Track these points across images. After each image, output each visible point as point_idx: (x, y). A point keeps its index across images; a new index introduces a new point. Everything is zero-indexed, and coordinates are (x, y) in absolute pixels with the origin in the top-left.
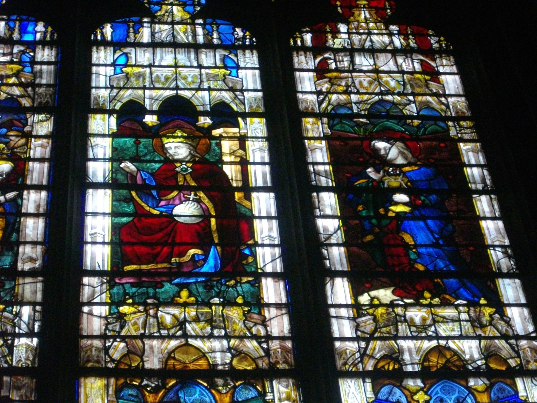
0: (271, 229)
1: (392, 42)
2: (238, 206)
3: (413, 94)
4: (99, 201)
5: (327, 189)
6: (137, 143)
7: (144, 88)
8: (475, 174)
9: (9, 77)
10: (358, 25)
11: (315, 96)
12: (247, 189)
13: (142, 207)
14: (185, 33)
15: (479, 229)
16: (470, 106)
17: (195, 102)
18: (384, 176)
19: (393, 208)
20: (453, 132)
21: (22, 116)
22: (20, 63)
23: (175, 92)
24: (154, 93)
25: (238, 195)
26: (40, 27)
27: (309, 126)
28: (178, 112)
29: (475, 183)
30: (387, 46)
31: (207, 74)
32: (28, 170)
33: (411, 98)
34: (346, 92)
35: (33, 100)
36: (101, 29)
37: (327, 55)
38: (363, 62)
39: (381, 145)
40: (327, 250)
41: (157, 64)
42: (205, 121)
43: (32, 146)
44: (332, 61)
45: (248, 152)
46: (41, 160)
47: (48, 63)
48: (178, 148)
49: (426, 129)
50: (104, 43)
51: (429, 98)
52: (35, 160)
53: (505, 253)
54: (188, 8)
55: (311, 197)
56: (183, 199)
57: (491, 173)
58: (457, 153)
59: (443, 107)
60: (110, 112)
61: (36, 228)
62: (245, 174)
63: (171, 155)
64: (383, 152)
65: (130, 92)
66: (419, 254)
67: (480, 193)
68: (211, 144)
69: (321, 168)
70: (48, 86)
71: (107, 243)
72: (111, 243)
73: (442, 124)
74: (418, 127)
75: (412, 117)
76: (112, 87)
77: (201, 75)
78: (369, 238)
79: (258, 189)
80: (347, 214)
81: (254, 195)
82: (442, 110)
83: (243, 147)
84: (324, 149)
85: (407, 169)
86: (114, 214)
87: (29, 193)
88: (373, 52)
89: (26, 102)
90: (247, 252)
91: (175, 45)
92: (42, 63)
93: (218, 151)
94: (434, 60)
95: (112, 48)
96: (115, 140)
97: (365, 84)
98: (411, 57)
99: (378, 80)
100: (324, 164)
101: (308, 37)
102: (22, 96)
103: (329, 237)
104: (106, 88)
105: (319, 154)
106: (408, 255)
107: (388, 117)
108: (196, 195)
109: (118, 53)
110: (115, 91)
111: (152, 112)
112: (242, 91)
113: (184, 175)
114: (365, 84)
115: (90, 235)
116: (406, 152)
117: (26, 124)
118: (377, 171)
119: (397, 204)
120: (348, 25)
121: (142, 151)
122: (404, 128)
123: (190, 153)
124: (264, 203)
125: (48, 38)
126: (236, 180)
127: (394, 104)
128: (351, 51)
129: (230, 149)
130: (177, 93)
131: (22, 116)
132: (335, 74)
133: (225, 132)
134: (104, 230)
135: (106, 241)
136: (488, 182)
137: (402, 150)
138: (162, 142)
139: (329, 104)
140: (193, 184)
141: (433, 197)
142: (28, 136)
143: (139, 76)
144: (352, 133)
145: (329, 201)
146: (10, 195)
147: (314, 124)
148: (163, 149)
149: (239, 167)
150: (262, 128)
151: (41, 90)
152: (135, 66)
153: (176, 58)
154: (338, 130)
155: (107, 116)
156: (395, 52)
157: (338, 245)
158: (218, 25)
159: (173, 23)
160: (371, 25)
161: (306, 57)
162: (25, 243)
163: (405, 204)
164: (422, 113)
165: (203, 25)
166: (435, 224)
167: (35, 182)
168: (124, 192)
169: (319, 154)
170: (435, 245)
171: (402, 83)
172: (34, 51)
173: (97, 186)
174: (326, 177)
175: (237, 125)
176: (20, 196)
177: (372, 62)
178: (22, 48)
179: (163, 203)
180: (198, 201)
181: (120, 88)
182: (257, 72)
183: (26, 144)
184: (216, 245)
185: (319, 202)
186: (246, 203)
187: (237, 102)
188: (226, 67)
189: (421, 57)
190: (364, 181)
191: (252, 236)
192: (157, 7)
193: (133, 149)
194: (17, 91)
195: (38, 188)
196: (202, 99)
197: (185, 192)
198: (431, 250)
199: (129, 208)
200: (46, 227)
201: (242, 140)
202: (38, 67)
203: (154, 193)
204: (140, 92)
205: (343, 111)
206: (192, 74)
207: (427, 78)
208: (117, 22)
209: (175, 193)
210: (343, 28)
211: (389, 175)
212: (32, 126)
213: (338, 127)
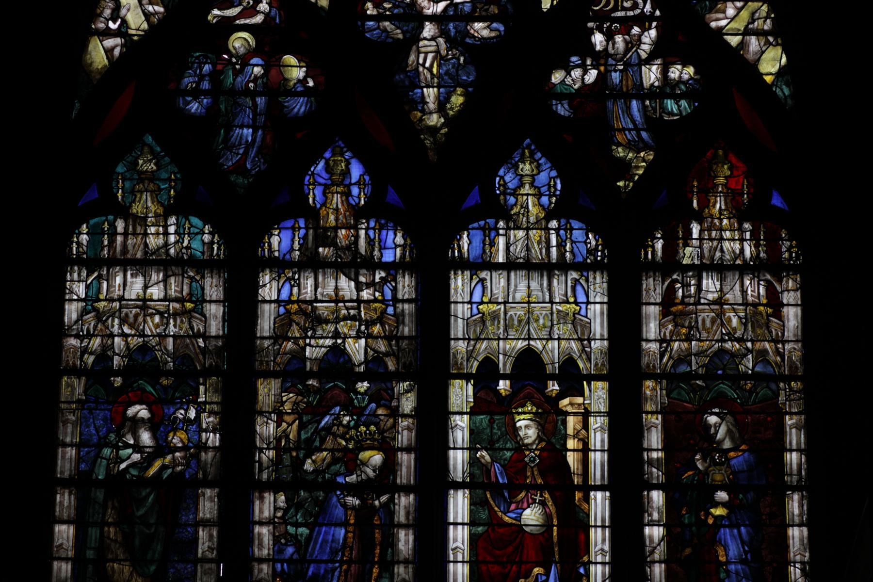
0: (604, 540)
1: (742, 250)
2: (577, 509)
3: (752, 341)
4: (459, 505)
5: (657, 487)
6: (491, 422)
7: (499, 339)
8: (793, 458)
9: (373, 323)
10: (712, 222)
11: (658, 344)
12: (587, 488)
13: (495, 511)
14: (539, 243)
15: (785, 537)
16: (805, 358)
17: (546, 358)
18: (710, 466)
19: (712, 510)
20: (782, 398)
21: (389, 385)
22: (383, 301)
23: (526, 343)
24: (509, 345)
25: (578, 495)
26: (399, 240)
27: (648, 392)
28: (529, 363)
29: (791, 475)
30: (736, 258)
31: (559, 311)
32: (398, 463)
33: (749, 345)
34: (688, 339)
35: (398, 359)
36: (459, 241)
37: (675, 277)
38: (710, 285)
39: (713, 419)
40: (650, 568)
41: (510, 300)
42: (553, 387)
43: (400, 429)
44: (679, 285)
45: (590, 443)
46: (407, 450)
47: (409, 301)
48: (527, 428)
49: (757, 394)
50: (463, 264)
51: (767, 345)
52: (402, 450)
53: (803, 570)
54: (545, 200)
55: (642, 496)
56: (530, 501)
57: (807, 461)
58: (780, 431)
59: (778, 358)
60: (467, 377)
61: (407, 542)
62: (585, 462)
63: (521, 439)
64: (713, 430)
65: (485, 344)
66: (728, 572)
67: (794, 489)
68: (557, 420)
69: (654, 455)
70: (409, 338)
71: (467, 562)
72: (470, 562)
73: (773, 386)
74: (750, 391)
75: (745, 376)
76: (469, 339)
77: (552, 308)
78: (688, 551)
79: (597, 488)
80: (671, 523)
81: (592, 493)
82: (776, 363)
83: (586, 426)
84: (660, 427)
85: (732, 454)
86: (472, 523)
87: (399, 496)
88: (720, 269)
89: (391, 365)
90: (582, 571)
91: (528, 266)
92: (403, 301)
93: (563, 432)
94: (780, 281)
95: (467, 273)
96: (474, 418)
97: (708, 323)
98: (758, 277)
99: (721, 314)
100: (657, 450)
101: (659, 245)
102: (387, 354)
103: (652, 552)
104: (464, 339)
105: (654, 439)
106: (718, 574)
107: (725, 377)
108: (541, 496)
109: (475, 280)
110: (472, 342)
111: (505, 377)
112: (589, 340)
113: (532, 468)
114: (708, 323)
115: (453, 550)
116: (734, 429)
117: (392, 397)
118: (704, 459)
119: (716, 505)
120: (701, 223)
121: (496, 434)
122: (737, 394)
123: (538, 436)
124: (599, 505)
125: (408, 259)
126: (578, 474)
127: (733, 355)
128: (699, 270)
129: (575, 429)
130: (529, 344)
131: (389, 385)
132: (680, 307)
133: (571, 404)
134: (463, 544)
135: (466, 521)
136: (803, 473)
137: (731, 427)
138: (514, 419)
139: (670, 357)
140: (539, 481)
141: (751, 495)
142: (395, 413)
143: (495, 316)
144: (687, 402)
145: (657, 497)
146: (384, 498)
147: (654, 389)
148: (516, 430)
149: (581, 454)
150: (605, 397)
151: (404, 344)
152: (490, 302)
153: (529, 287)
154: (675, 399)
155: (464, 382)
156: (744, 269)
157: (660, 562)
158: (572, 229)
159: (528, 229)
160: (725, 221)
161: (654, 280)
162: (399, 562)
163: (724, 505)
164: (757, 369)
165: (557, 230)
166: (748, 532)
167: (404, 481)
168: (480, 492)
169: (654, 439)
170: (742, 561)
171: (744, 320)
172: (395, 280)
173: (457, 486)
174: (658, 469)
175: (582, 395)
176: (391, 500)
177: (718, 284)
178: (383, 274)
179: (513, 507)
180: (543, 503)
181: (478, 339)
182: (605, 306)
183: (395, 425)
184: (556, 563)
185: (648, 503)
186: (585, 506)
187: (584, 357)
188: (576, 303)
189: (769, 277)
190: (691, 473)
191: (587, 552)
192: (512, 200)
193: (488, 430)
194: (382, 346)
195: (406, 489)
196: (552, 352)
197: (533, 492)
198: (739, 567)
199: (484, 515)
200: (415, 540)
201: (586, 415)
202: (400, 306)
203: (506, 494)
204: (495, 343)
205: (683, 368)
206: (544, 313)
207: (770, 310)
208: (473, 229)
209: (523, 494)
210: (695, 229)
211: (716, 464)
212: (398, 400)
213: (674, 395)
